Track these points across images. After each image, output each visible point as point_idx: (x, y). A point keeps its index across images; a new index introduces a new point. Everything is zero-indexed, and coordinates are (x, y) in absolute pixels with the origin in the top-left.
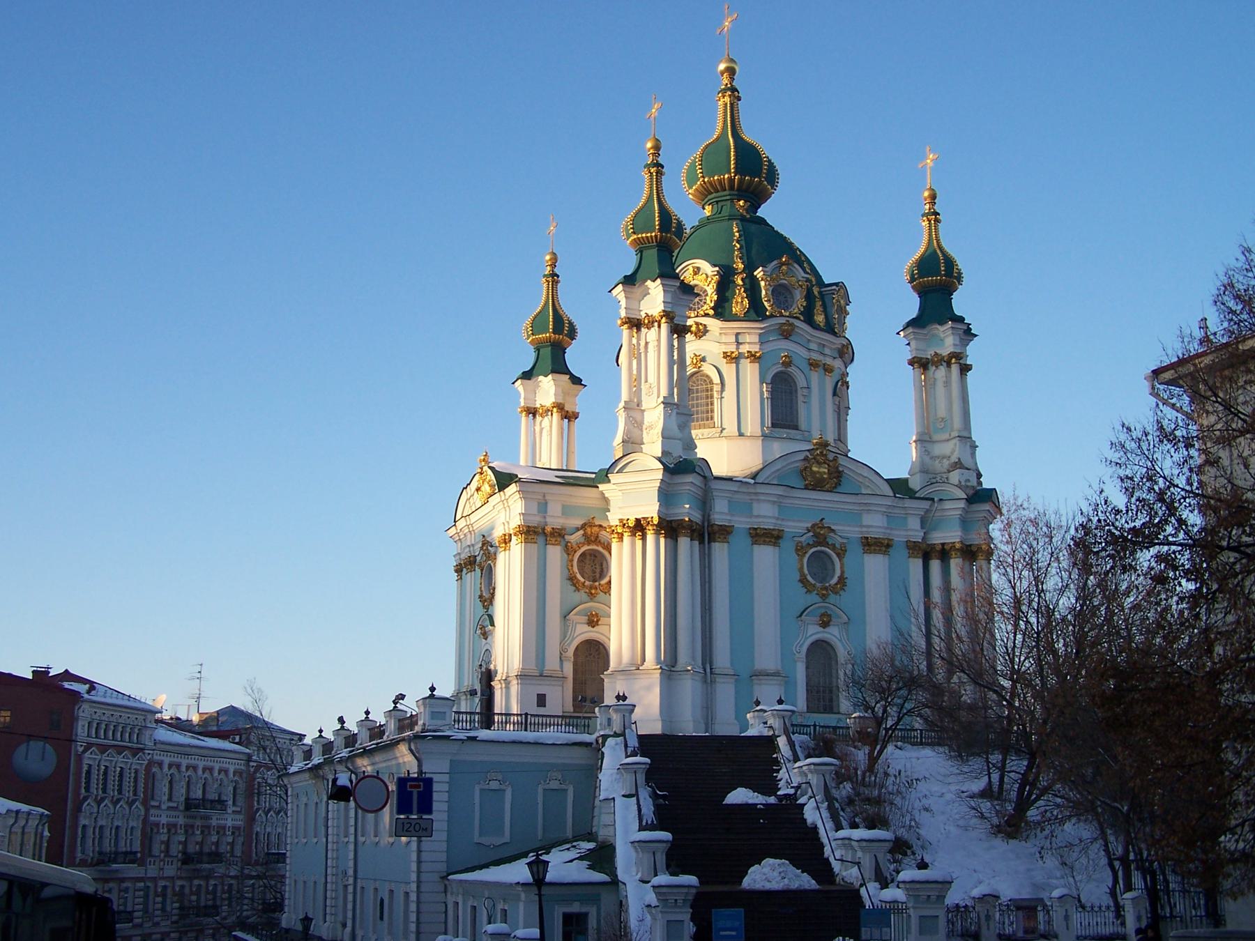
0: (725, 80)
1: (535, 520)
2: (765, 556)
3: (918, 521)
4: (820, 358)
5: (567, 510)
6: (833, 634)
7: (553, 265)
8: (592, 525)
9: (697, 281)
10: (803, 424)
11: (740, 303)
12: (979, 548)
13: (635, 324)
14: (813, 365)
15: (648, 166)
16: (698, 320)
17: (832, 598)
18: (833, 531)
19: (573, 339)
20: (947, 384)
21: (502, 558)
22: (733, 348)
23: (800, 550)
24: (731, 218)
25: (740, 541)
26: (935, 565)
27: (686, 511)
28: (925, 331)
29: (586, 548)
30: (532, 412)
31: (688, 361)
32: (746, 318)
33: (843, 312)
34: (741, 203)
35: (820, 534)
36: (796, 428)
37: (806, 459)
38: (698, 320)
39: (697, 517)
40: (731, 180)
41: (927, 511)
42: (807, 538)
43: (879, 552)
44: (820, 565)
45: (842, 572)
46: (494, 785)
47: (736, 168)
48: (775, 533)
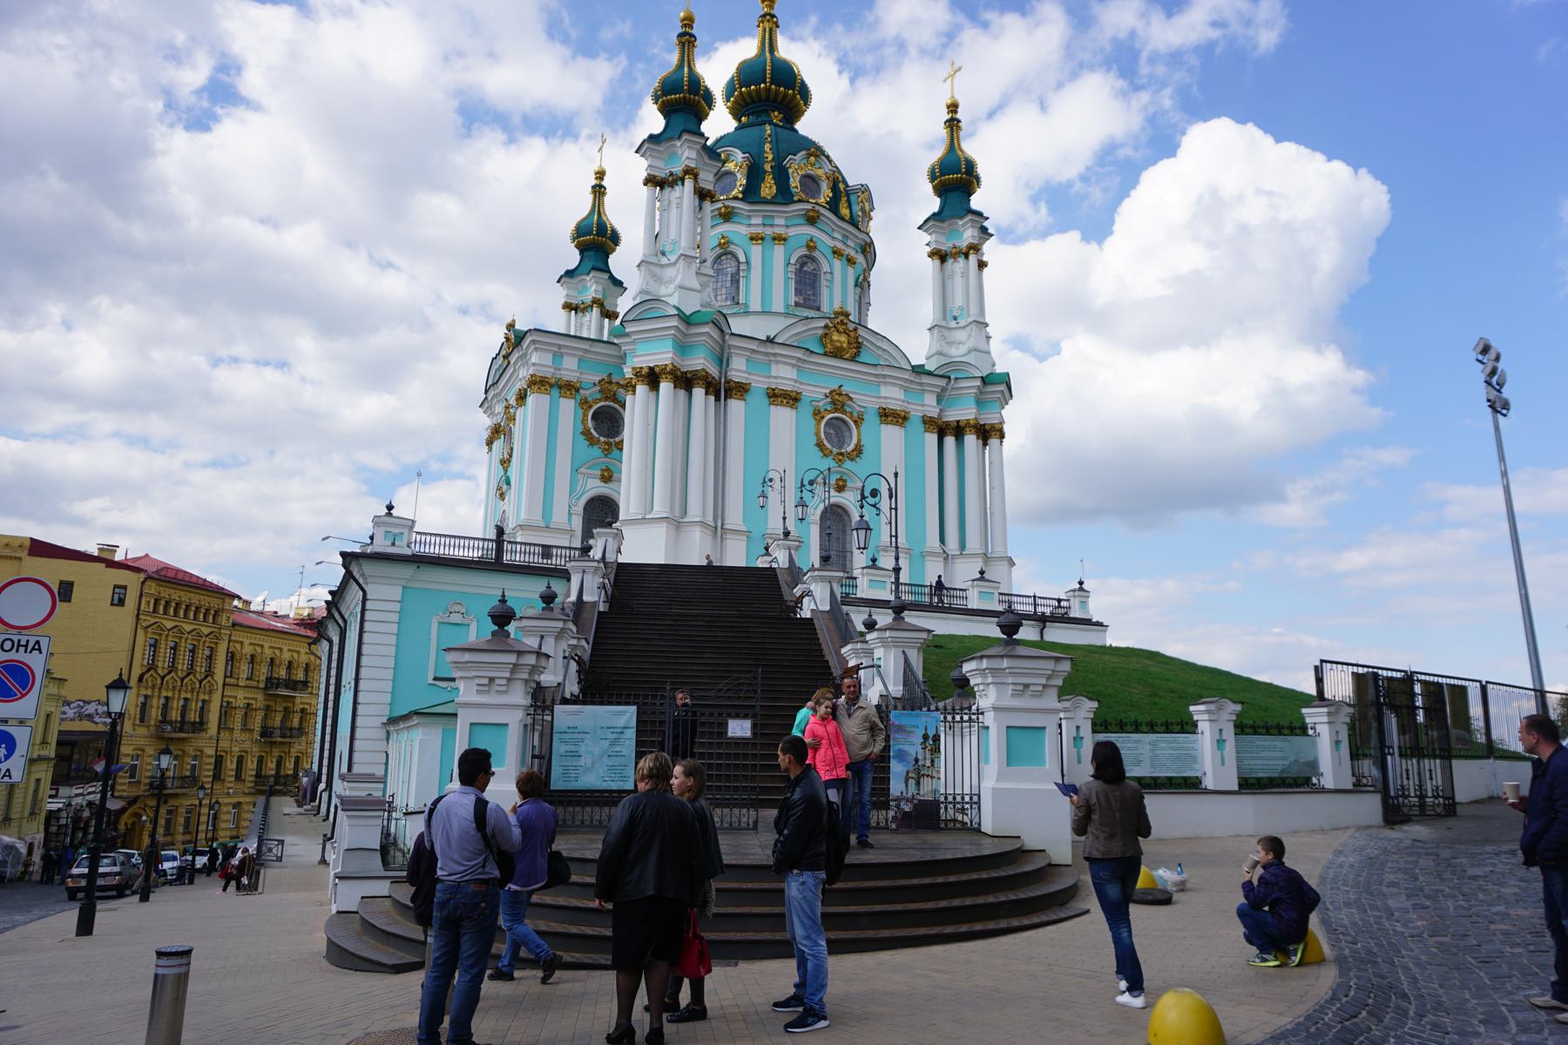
1: (547, 372)
6: (849, 499)
7: (601, 179)
8: (610, 383)
11: (768, 188)
12: (993, 427)
17: (848, 464)
20: (965, 275)
21: (519, 413)
22: (759, 230)
23: (818, 414)
25: (757, 398)
26: (950, 441)
27: (699, 361)
33: (867, 216)
35: (838, 400)
36: (818, 309)
37: (826, 327)
39: (713, 371)
40: (768, 90)
41: (944, 389)
42: (823, 404)
43: (897, 423)
44: (838, 430)
46: (456, 618)
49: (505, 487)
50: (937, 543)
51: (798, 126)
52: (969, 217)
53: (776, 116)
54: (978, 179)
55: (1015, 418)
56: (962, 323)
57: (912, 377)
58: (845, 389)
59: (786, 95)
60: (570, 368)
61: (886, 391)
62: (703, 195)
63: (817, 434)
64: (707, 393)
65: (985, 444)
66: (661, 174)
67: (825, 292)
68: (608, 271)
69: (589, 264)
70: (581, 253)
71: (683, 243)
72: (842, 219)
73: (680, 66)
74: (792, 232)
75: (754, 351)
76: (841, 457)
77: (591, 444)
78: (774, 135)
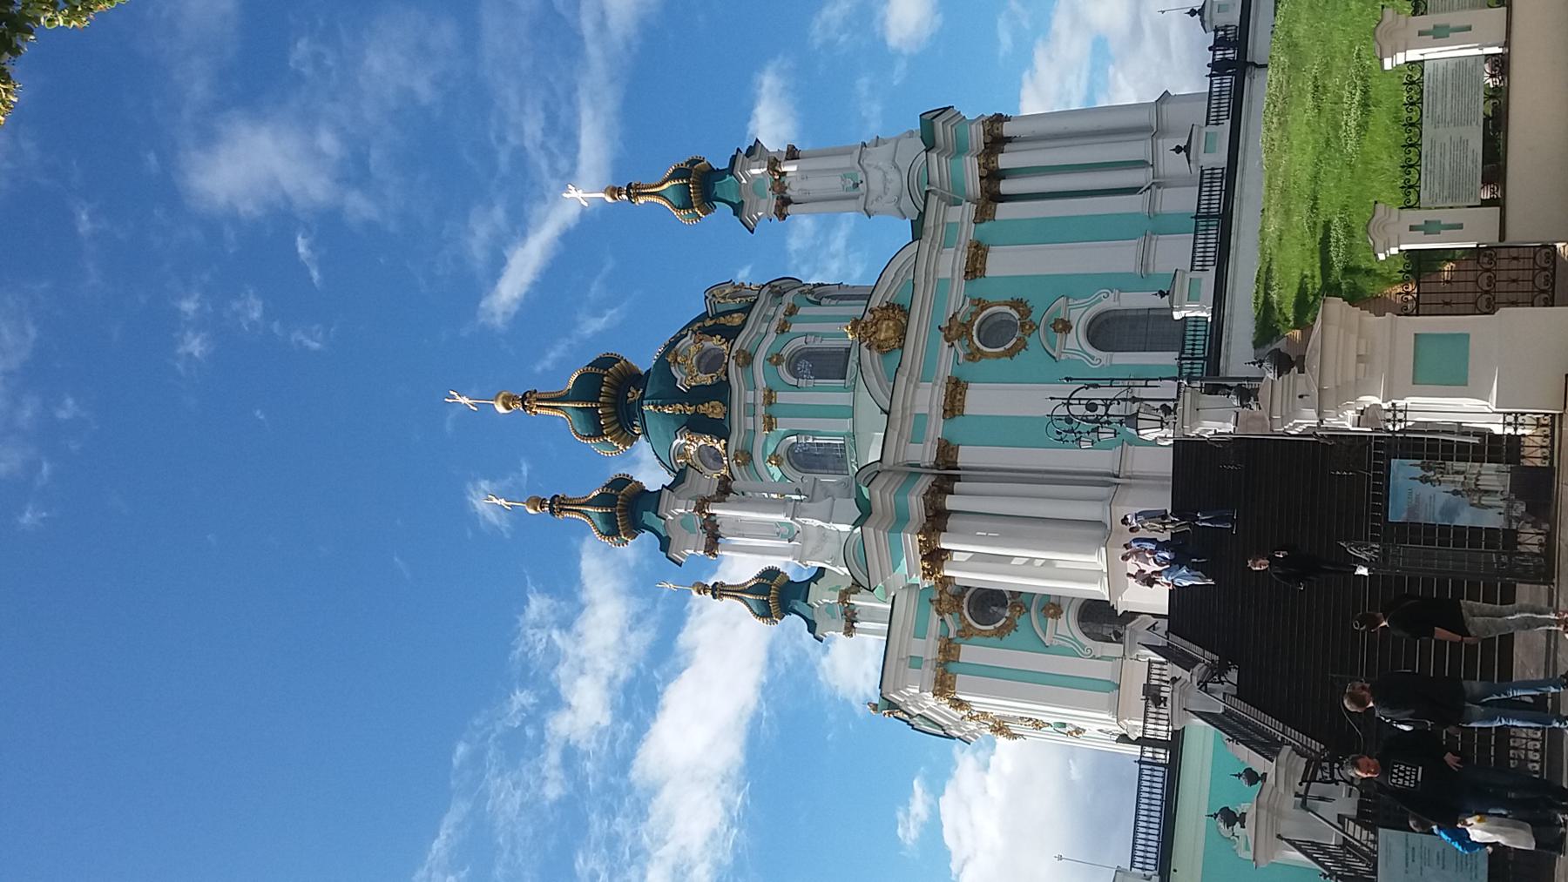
2: (978, 400)
5: (920, 633)
6: (1080, 317)
7: (705, 588)
8: (940, 601)
11: (713, 410)
14: (783, 329)
17: (1034, 317)
19: (778, 572)
21: (977, 708)
23: (974, 355)
26: (1006, 187)
28: (747, 201)
32: (727, 403)
35: (955, 331)
37: (869, 347)
38: (731, 456)
39: (925, 483)
41: (942, 198)
43: (984, 257)
44: (995, 332)
45: (1006, 304)
49: (1069, 729)
50: (1137, 197)
51: (643, 371)
53: (633, 395)
54: (693, 162)
55: (974, 108)
56: (861, 176)
57: (927, 237)
58: (945, 324)
59: (610, 385)
60: (928, 648)
61: (945, 271)
62: (725, 490)
63: (998, 356)
65: (1009, 140)
66: (703, 538)
67: (829, 343)
69: (799, 605)
71: (781, 518)
72: (745, 322)
73: (586, 515)
74: (761, 383)
76: (1028, 326)
77: (1015, 628)
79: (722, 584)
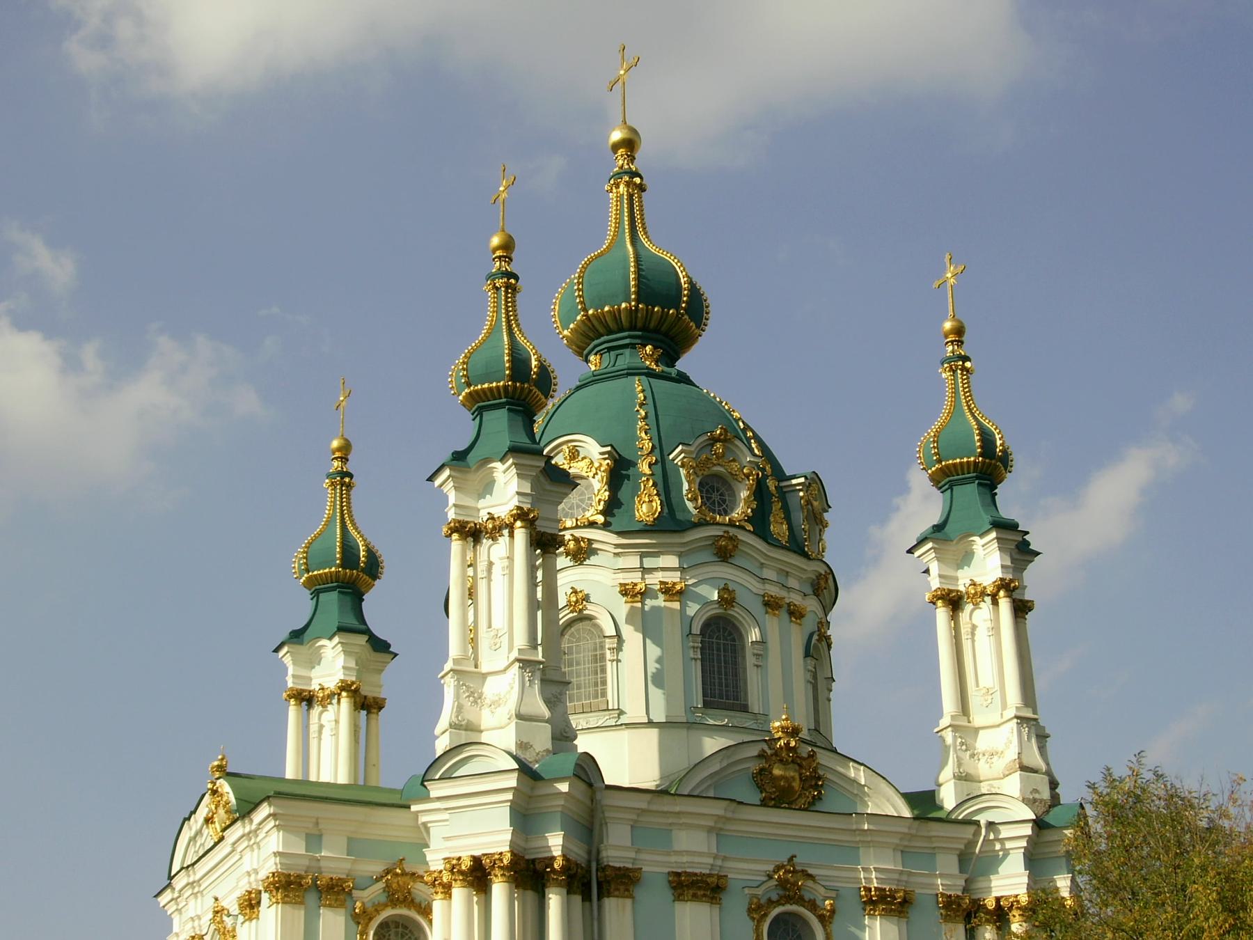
0: (621, 161)
3: (954, 860)
4: (783, 593)
5: (354, 846)
7: (344, 459)
9: (576, 468)
10: (755, 705)
13: (472, 533)
14: (771, 604)
15: (492, 277)
16: (579, 533)
18: (811, 877)
22: (635, 577)
23: (757, 910)
24: (632, 372)
29: (388, 913)
30: (306, 699)
31: (562, 602)
33: (817, 520)
34: (648, 348)
35: (791, 883)
36: (744, 708)
37: (762, 755)
38: (579, 533)
39: (579, 854)
47: (638, 293)
48: (714, 880)
52: (993, 535)
60: (333, 858)
64: (569, 893)
67: (753, 678)
68: (367, 632)
70: (316, 594)
71: (521, 640)
75: (643, 811)
78: (652, 400)
79: (349, 486)
